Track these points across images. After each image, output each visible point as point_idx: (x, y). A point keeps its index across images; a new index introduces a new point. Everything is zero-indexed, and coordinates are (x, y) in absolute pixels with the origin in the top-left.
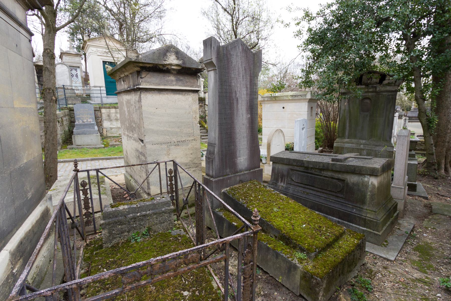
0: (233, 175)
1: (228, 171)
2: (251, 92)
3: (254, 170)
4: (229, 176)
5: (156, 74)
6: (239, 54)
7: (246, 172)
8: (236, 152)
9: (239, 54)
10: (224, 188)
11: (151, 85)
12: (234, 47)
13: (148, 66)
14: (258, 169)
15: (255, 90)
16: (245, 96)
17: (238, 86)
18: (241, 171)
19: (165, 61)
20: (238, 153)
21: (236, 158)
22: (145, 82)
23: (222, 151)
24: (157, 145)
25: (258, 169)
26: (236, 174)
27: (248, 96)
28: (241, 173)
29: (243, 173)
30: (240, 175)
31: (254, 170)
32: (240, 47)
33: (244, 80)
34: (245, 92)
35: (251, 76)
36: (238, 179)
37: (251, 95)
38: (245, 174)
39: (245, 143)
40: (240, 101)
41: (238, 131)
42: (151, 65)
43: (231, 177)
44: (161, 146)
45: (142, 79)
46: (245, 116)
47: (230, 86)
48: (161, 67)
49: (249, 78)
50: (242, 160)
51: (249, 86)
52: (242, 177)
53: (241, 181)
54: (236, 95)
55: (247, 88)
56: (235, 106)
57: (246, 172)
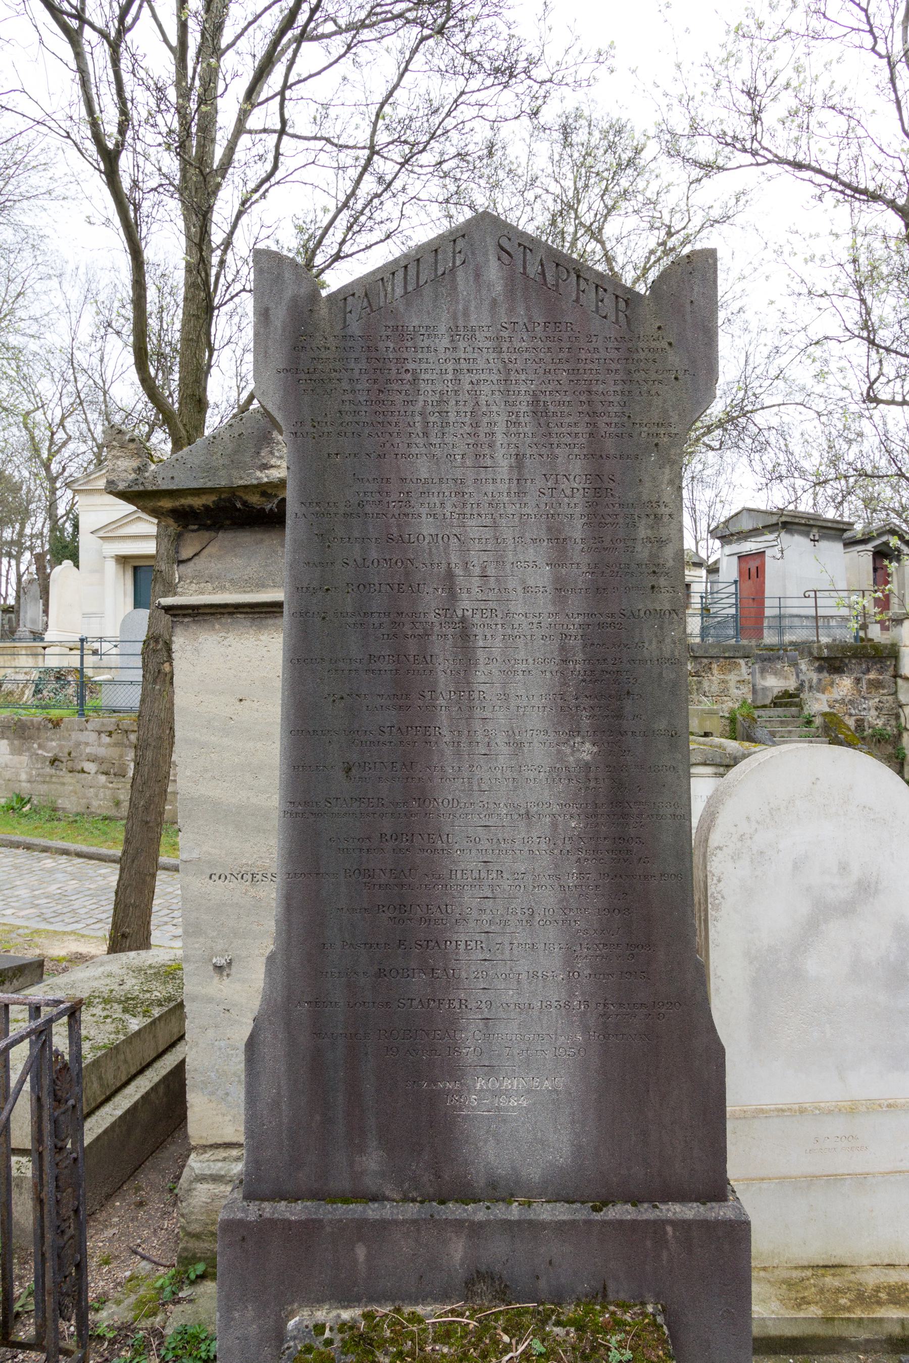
0: (411, 1210)
1: (372, 1161)
2: (596, 568)
3: (645, 1213)
4: (373, 1211)
5: (246, 538)
6: (480, 317)
7: (546, 1212)
8: (452, 1025)
9: (480, 317)
10: (319, 1301)
11: (223, 588)
12: (437, 279)
13: (197, 502)
14: (688, 1211)
15: (643, 553)
16: (544, 604)
17: (474, 533)
18: (500, 1191)
19: (265, 467)
20: (470, 1038)
21: (455, 1072)
22: (198, 577)
23: (318, 1003)
24: (233, 884)
25: (688, 1211)
26: (454, 1211)
27: (576, 603)
28: (500, 1212)
29: (514, 1211)
30: (475, 1230)
31: (645, 1213)
32: (493, 272)
33: (534, 486)
34: (541, 576)
35: (595, 456)
36: (457, 1251)
37: (598, 590)
38: (535, 1226)
39: (551, 962)
40: (489, 644)
41: (468, 861)
42: (208, 500)
43: (383, 1225)
44: (252, 892)
45: (182, 567)
46: (539, 753)
47: (397, 540)
48: (255, 499)
49: (577, 467)
50: (522, 1091)
51: (577, 530)
52: (497, 1250)
53: (481, 1282)
54: (452, 595)
55: (558, 540)
56: (443, 681)
57: (546, 1212)
